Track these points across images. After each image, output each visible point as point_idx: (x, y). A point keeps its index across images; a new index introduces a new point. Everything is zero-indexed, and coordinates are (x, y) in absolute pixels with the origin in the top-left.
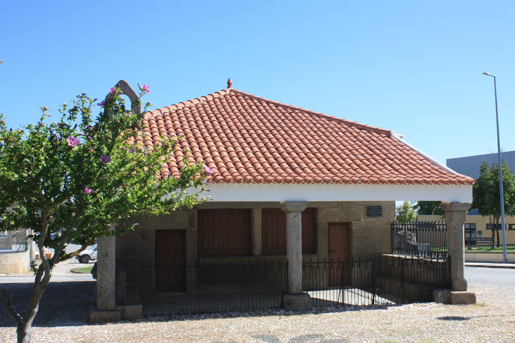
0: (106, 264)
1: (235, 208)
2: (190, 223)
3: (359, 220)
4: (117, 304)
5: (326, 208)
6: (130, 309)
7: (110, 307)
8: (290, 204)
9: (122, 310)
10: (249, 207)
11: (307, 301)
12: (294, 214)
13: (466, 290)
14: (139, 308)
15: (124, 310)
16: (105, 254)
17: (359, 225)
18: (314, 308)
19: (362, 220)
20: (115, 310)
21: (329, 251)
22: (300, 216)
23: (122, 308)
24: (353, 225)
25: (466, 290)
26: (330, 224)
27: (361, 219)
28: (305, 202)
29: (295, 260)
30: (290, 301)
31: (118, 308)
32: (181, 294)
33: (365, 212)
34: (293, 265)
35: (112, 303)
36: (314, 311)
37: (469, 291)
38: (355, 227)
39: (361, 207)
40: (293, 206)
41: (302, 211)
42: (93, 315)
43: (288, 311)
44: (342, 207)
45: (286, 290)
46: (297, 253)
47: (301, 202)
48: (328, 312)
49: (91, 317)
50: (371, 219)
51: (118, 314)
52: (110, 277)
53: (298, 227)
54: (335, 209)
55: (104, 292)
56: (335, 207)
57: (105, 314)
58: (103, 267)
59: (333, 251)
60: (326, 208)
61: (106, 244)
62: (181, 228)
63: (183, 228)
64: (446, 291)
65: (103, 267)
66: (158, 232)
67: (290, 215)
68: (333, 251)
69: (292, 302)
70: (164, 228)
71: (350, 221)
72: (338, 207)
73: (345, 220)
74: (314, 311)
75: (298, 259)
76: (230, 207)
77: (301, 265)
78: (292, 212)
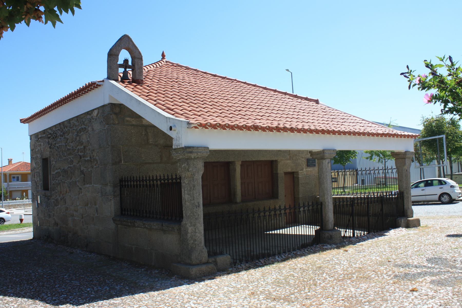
0: (198, 215)
3: (302, 170)
4: (209, 255)
13: (413, 217)
16: (197, 204)
19: (304, 170)
25: (413, 217)
33: (306, 164)
37: (415, 217)
39: (303, 159)
42: (194, 271)
50: (310, 169)
55: (198, 244)
58: (196, 219)
61: (198, 194)
64: (405, 219)
65: (196, 219)
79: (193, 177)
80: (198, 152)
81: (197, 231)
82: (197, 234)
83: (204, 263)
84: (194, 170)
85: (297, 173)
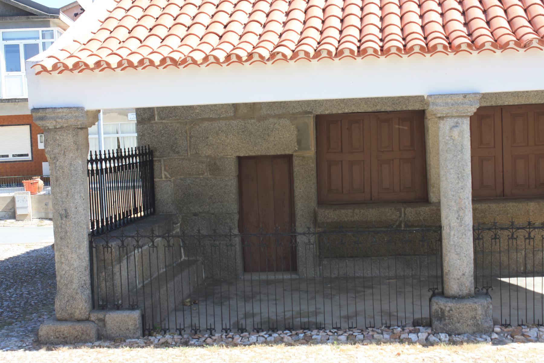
0: (66, 233)
1: (389, 109)
2: (299, 142)
6: (115, 319)
7: (77, 314)
8: (439, 101)
9: (100, 320)
10: (418, 107)
11: (480, 312)
12: (450, 122)
14: (132, 318)
15: (103, 320)
16: (63, 212)
18: (497, 329)
20: (88, 320)
22: (466, 126)
23: (101, 315)
28: (475, 94)
29: (454, 223)
30: (443, 311)
31: (93, 317)
32: (287, 276)
34: (449, 234)
35: (81, 305)
36: (495, 336)
40: (447, 104)
41: (470, 114)
42: (46, 329)
43: (435, 333)
45: (437, 287)
46: (460, 209)
47: (465, 96)
48: (527, 339)
49: (41, 333)
51: (91, 329)
52: (74, 256)
53: (461, 151)
55: (66, 285)
57: (65, 328)
58: (61, 238)
61: (64, 194)
62: (283, 153)
63: (287, 152)
66: (240, 159)
67: (441, 125)
69: (446, 314)
70: (251, 154)
74: (495, 336)
75: (461, 220)
76: (378, 108)
77: (470, 234)
78: (447, 117)
79: (55, 163)
80: (58, 117)
81: (63, 260)
82: (63, 266)
83: (79, 321)
84: (56, 151)
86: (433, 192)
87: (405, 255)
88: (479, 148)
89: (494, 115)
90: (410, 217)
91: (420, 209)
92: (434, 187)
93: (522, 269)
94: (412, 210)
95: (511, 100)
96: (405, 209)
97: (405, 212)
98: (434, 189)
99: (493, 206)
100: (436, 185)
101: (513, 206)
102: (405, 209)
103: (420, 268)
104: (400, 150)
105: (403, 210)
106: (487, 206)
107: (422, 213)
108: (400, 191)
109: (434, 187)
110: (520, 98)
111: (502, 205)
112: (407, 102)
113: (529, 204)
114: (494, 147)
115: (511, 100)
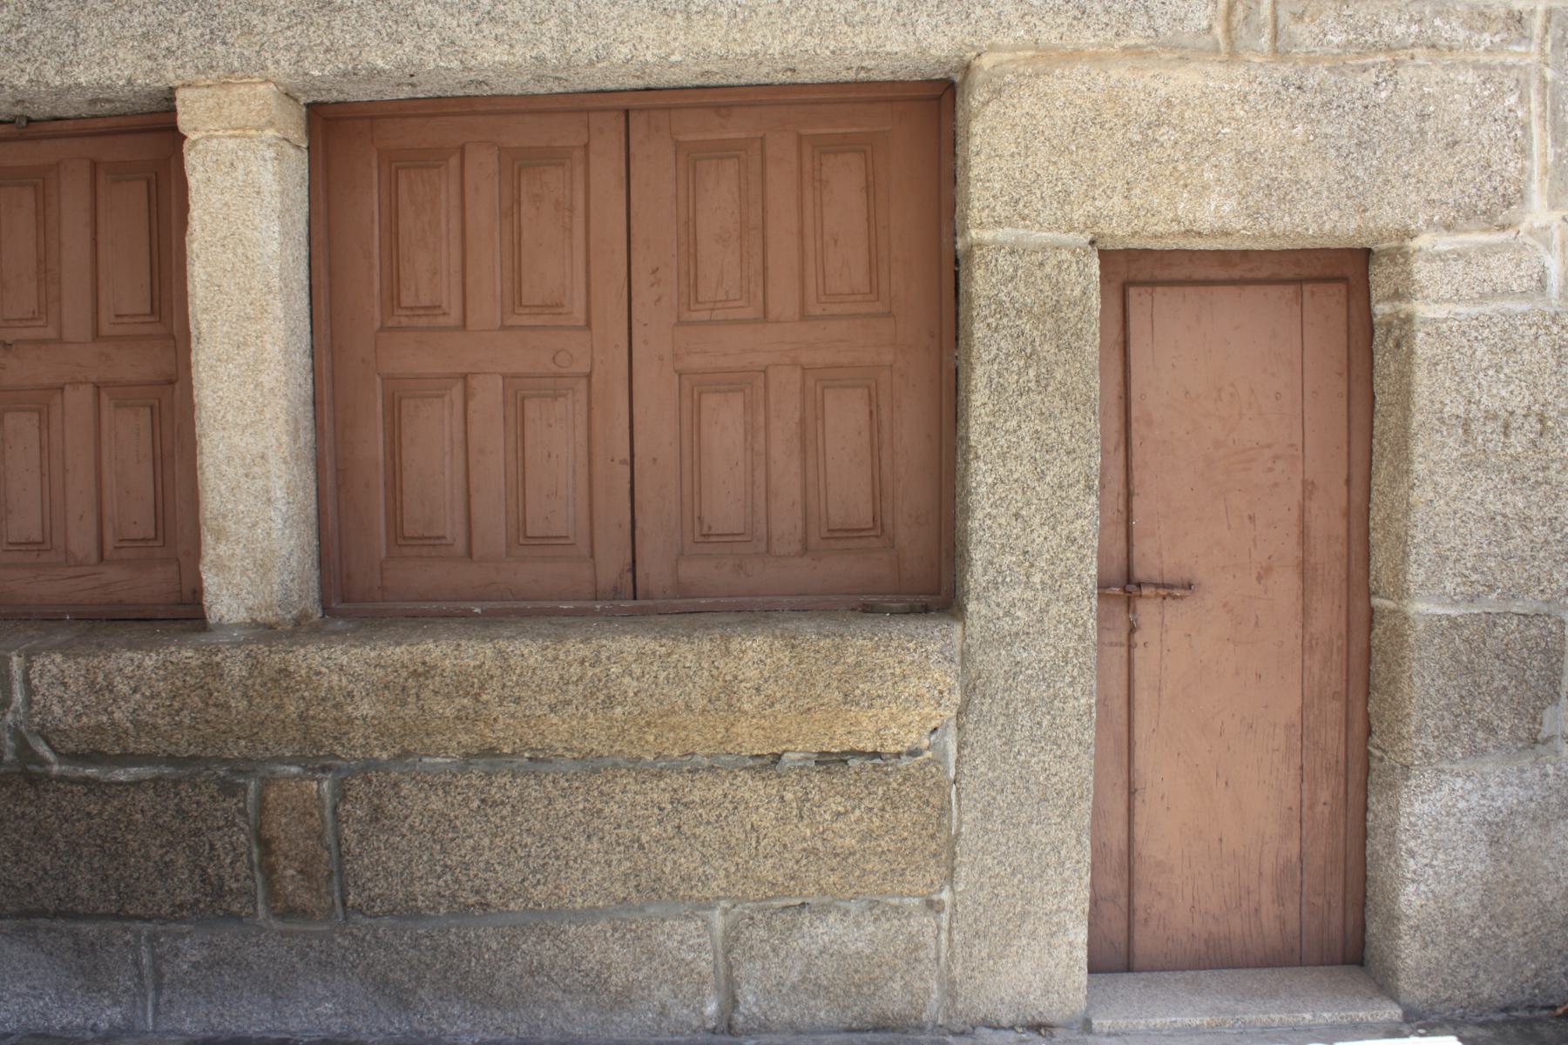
3: (1496, 209)
5: (1074, 55)
17: (1500, 270)
21: (1124, 586)
24: (1422, 271)
26: (1132, 273)
27: (1514, 197)
38: (1439, 298)
39: (1524, 55)
44: (1279, 52)
54: (1187, 79)
56: (1183, 54)
59: (1175, 589)
60: (1074, 55)
68: (1175, 589)
71: (1386, 217)
72: (1233, 56)
73: (1316, 219)
85: (1400, 256)
86: (220, 567)
87: (74, 916)
88: (503, 327)
89: (586, 146)
90: (57, 710)
91: (111, 665)
92: (220, 535)
93: (711, 1008)
94: (70, 667)
95: (649, 34)
96: (29, 656)
97: (27, 681)
98: (222, 549)
99: (528, 651)
100: (231, 525)
101: (640, 656)
102: (29, 656)
103: (158, 988)
104: (97, 335)
105: (16, 663)
106: (488, 649)
107: (123, 688)
108: (101, 558)
109: (220, 535)
110: (699, 23)
111: (575, 648)
112: (67, 39)
113: (734, 645)
114: (588, 325)
115: (649, 34)
